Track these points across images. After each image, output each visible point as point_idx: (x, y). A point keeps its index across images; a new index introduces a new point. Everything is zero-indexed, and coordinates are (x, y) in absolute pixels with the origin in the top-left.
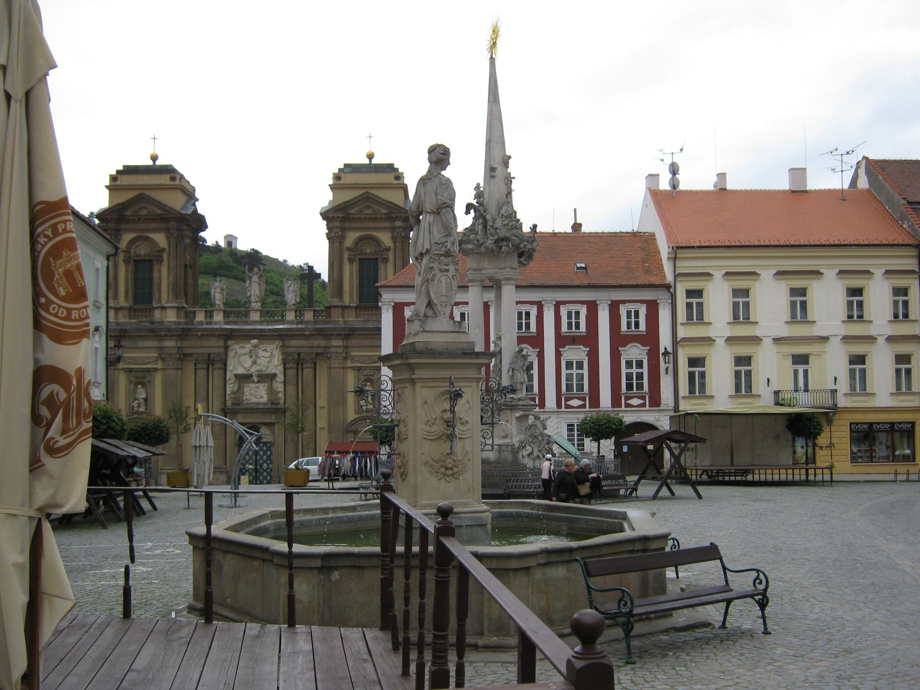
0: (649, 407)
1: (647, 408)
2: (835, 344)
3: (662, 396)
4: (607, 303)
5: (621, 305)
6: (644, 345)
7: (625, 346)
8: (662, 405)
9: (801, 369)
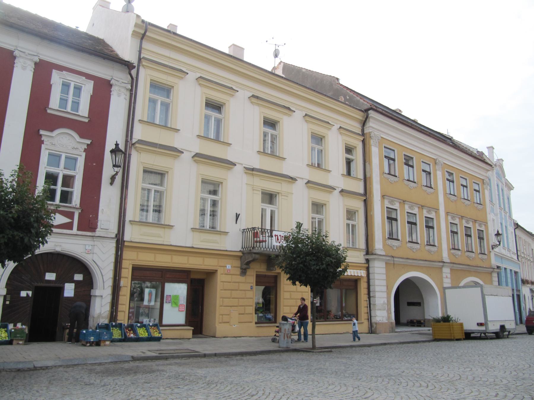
0: (79, 229)
1: (75, 230)
2: (299, 187)
3: (101, 216)
4: (32, 60)
5: (54, 71)
6: (82, 136)
7: (51, 129)
8: (97, 230)
9: (269, 208)
